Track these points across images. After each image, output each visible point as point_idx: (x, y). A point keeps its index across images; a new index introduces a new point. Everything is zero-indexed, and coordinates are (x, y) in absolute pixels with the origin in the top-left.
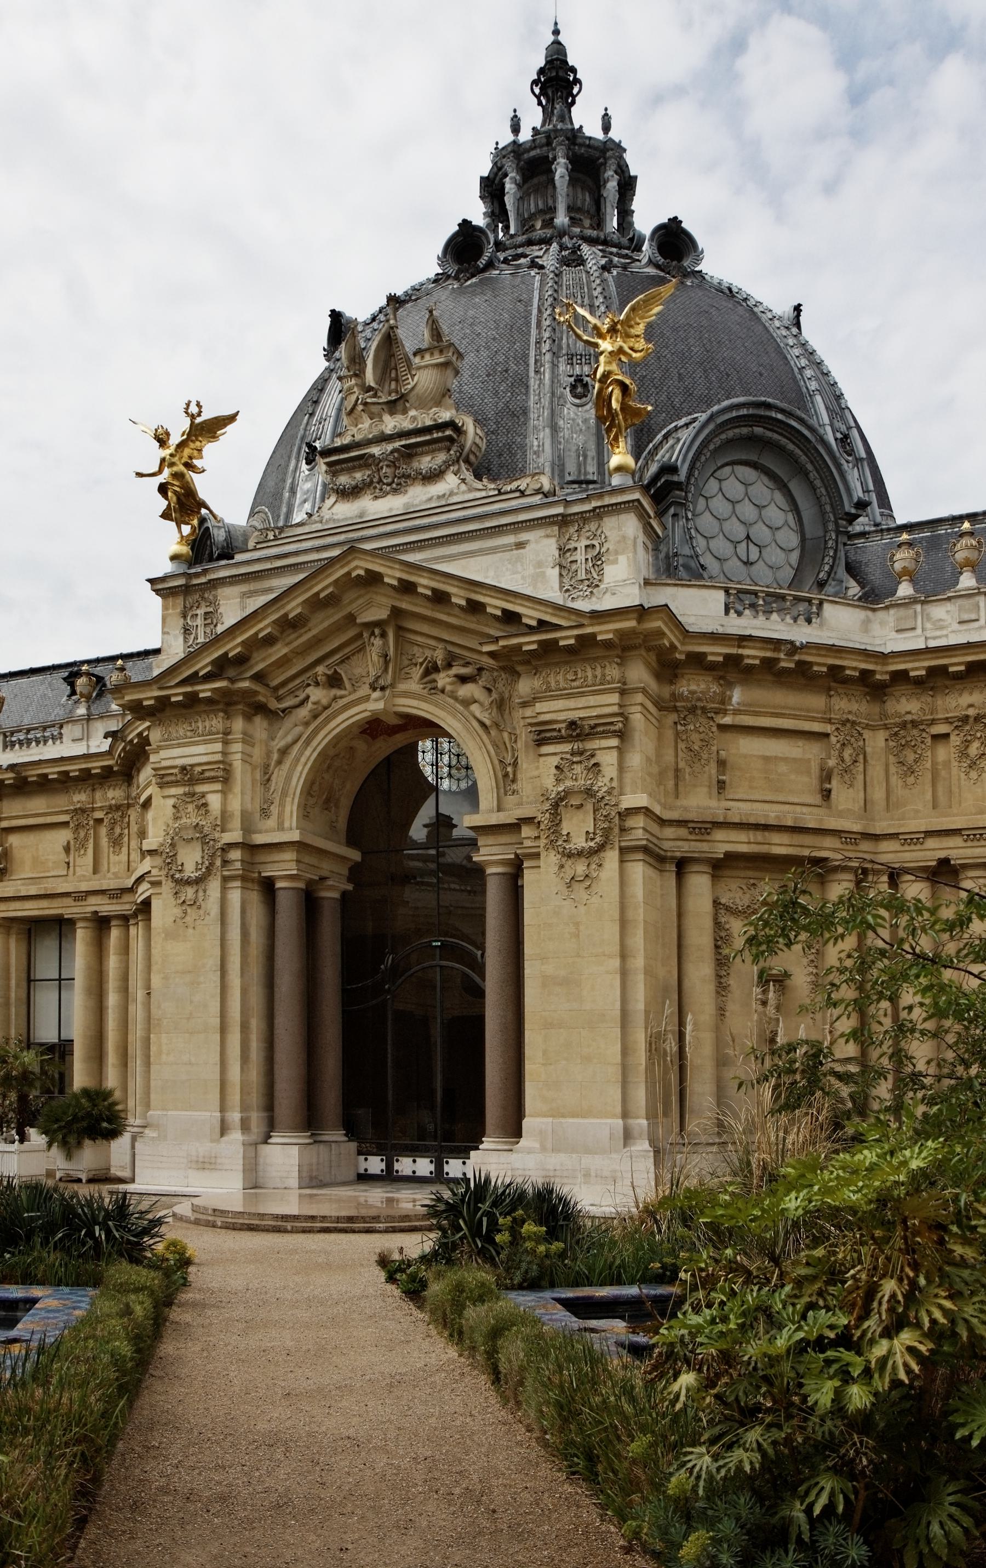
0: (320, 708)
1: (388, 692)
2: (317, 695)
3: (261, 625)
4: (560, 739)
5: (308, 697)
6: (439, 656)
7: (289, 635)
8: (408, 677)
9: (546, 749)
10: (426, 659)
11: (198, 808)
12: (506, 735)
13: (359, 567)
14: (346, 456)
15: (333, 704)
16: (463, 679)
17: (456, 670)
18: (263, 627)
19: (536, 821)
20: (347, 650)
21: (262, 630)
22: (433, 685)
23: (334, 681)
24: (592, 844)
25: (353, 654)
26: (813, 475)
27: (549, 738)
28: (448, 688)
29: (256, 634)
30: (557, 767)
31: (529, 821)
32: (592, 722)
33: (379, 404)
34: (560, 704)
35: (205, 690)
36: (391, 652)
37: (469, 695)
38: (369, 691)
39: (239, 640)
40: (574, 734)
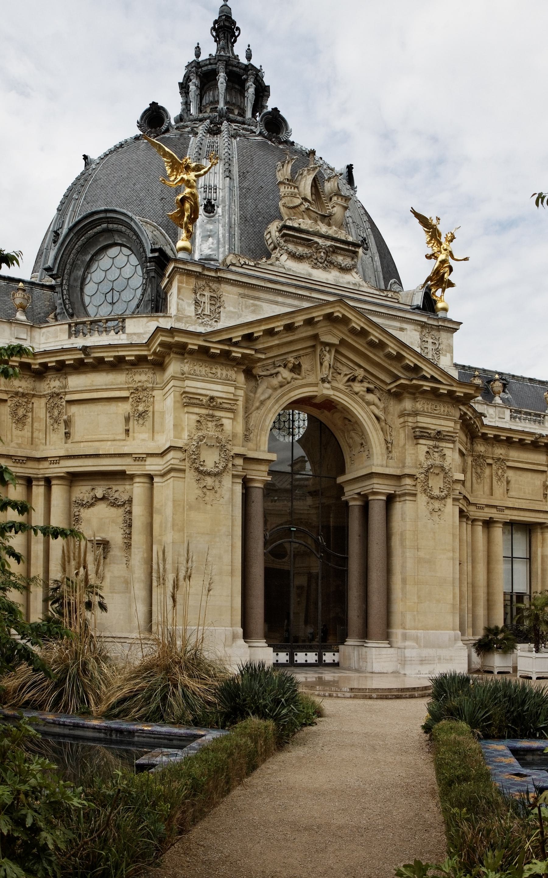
0: (286, 382)
2: (286, 374)
4: (429, 438)
5: (277, 373)
6: (360, 373)
9: (421, 441)
13: (339, 311)
14: (298, 235)
15: (293, 383)
16: (369, 390)
17: (366, 385)
18: (279, 325)
20: (301, 352)
23: (296, 369)
25: (303, 356)
27: (425, 436)
30: (428, 452)
33: (317, 213)
34: (428, 420)
37: (372, 400)
38: (320, 382)
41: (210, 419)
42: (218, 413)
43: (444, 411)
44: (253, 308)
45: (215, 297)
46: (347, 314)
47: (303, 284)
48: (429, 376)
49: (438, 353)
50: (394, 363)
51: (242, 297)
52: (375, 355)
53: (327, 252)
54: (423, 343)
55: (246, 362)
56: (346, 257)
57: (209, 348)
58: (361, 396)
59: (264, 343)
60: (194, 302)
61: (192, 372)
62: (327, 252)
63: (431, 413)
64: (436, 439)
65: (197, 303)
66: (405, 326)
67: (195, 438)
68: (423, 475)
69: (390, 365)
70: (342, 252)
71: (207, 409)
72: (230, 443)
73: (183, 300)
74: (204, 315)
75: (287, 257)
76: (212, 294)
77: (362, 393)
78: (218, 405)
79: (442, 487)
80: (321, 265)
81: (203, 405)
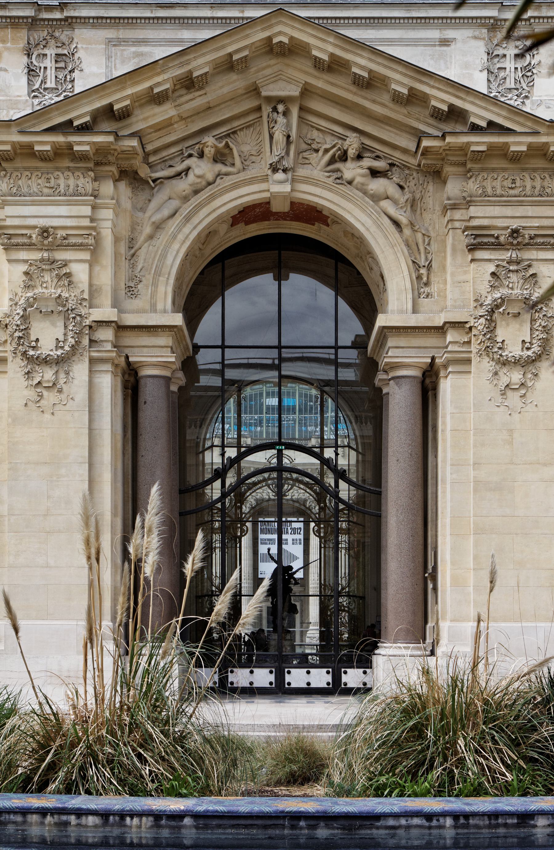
1: (290, 175)
3: (159, 79)
4: (498, 246)
7: (181, 96)
8: (306, 162)
10: (334, 146)
11: (59, 278)
12: (419, 236)
16: (374, 173)
17: (367, 162)
19: (468, 326)
21: (158, 84)
22: (339, 175)
24: (530, 353)
27: (486, 244)
28: (358, 180)
30: (493, 274)
31: (458, 325)
32: (533, 232)
34: (497, 211)
37: (382, 190)
40: (515, 242)
41: (47, 267)
43: (534, 187)
45: (65, 55)
46: (297, 35)
48: (484, 124)
49: (529, 74)
50: (415, 110)
51: (115, 45)
52: (374, 101)
54: (496, 60)
55: (111, 159)
58: (359, 186)
59: (145, 119)
60: (26, 71)
63: (502, 196)
64: (512, 244)
65: (33, 70)
66: (450, 34)
67: (22, 301)
68: (482, 320)
69: (409, 115)
71: (42, 249)
73: (6, 70)
74: (45, 89)
76: (60, 51)
77: (358, 180)
78: (59, 242)
79: (528, 339)
81: (34, 245)
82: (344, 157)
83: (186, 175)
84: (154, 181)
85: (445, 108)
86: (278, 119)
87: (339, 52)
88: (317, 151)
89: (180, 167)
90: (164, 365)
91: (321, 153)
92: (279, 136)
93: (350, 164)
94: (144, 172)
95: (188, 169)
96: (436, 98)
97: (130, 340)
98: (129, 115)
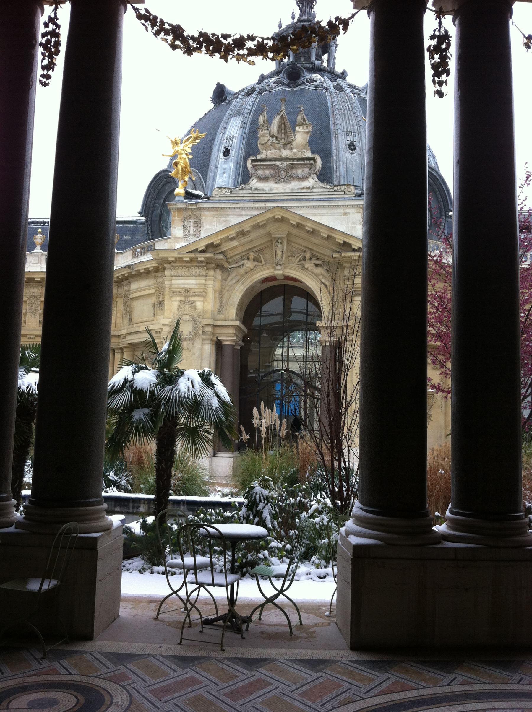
1: (283, 266)
3: (231, 233)
7: (240, 238)
16: (317, 265)
18: (232, 233)
21: (231, 235)
26: (438, 193)
28: (310, 268)
29: (228, 236)
35: (201, 257)
36: (285, 250)
39: (220, 238)
42: (192, 299)
44: (224, 223)
47: (263, 198)
48: (356, 248)
51: (216, 217)
53: (286, 170)
55: (212, 261)
56: (304, 169)
57: (182, 258)
59: (226, 246)
60: (183, 227)
61: (176, 274)
62: (286, 170)
66: (348, 211)
70: (301, 166)
72: (201, 317)
74: (190, 234)
75: (256, 181)
76: (196, 220)
77: (310, 268)
80: (282, 180)
82: (305, 259)
83: (243, 266)
84: (230, 269)
85: (342, 242)
86: (279, 245)
87: (300, 222)
88: (294, 256)
89: (240, 264)
90: (232, 341)
91: (296, 257)
92: (279, 252)
93: (307, 261)
94: (226, 265)
95: (243, 265)
96: (338, 239)
97: (218, 331)
98: (220, 246)
